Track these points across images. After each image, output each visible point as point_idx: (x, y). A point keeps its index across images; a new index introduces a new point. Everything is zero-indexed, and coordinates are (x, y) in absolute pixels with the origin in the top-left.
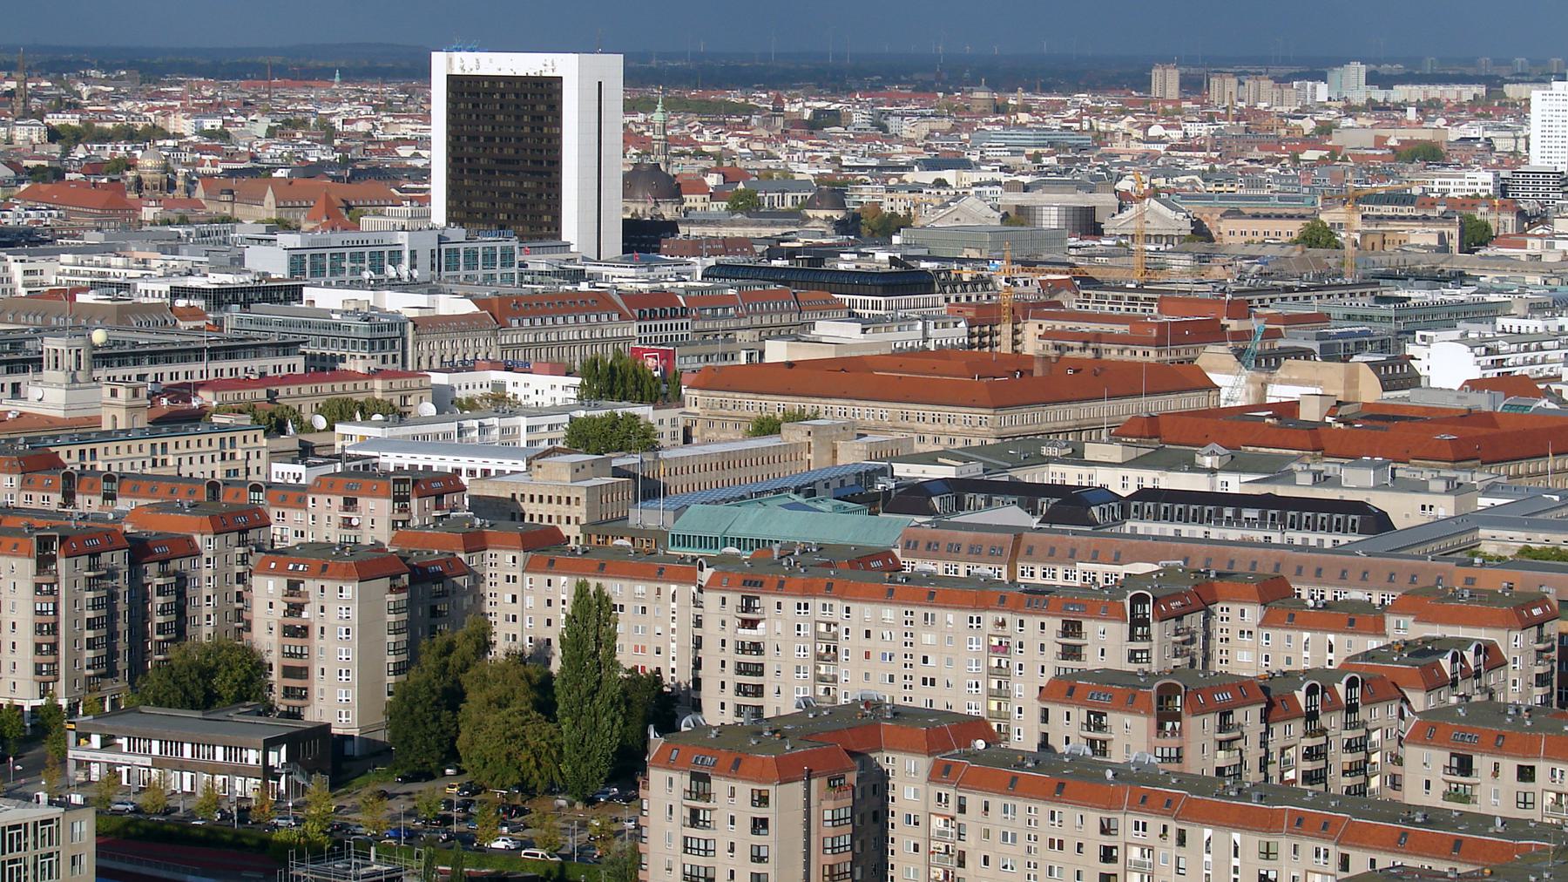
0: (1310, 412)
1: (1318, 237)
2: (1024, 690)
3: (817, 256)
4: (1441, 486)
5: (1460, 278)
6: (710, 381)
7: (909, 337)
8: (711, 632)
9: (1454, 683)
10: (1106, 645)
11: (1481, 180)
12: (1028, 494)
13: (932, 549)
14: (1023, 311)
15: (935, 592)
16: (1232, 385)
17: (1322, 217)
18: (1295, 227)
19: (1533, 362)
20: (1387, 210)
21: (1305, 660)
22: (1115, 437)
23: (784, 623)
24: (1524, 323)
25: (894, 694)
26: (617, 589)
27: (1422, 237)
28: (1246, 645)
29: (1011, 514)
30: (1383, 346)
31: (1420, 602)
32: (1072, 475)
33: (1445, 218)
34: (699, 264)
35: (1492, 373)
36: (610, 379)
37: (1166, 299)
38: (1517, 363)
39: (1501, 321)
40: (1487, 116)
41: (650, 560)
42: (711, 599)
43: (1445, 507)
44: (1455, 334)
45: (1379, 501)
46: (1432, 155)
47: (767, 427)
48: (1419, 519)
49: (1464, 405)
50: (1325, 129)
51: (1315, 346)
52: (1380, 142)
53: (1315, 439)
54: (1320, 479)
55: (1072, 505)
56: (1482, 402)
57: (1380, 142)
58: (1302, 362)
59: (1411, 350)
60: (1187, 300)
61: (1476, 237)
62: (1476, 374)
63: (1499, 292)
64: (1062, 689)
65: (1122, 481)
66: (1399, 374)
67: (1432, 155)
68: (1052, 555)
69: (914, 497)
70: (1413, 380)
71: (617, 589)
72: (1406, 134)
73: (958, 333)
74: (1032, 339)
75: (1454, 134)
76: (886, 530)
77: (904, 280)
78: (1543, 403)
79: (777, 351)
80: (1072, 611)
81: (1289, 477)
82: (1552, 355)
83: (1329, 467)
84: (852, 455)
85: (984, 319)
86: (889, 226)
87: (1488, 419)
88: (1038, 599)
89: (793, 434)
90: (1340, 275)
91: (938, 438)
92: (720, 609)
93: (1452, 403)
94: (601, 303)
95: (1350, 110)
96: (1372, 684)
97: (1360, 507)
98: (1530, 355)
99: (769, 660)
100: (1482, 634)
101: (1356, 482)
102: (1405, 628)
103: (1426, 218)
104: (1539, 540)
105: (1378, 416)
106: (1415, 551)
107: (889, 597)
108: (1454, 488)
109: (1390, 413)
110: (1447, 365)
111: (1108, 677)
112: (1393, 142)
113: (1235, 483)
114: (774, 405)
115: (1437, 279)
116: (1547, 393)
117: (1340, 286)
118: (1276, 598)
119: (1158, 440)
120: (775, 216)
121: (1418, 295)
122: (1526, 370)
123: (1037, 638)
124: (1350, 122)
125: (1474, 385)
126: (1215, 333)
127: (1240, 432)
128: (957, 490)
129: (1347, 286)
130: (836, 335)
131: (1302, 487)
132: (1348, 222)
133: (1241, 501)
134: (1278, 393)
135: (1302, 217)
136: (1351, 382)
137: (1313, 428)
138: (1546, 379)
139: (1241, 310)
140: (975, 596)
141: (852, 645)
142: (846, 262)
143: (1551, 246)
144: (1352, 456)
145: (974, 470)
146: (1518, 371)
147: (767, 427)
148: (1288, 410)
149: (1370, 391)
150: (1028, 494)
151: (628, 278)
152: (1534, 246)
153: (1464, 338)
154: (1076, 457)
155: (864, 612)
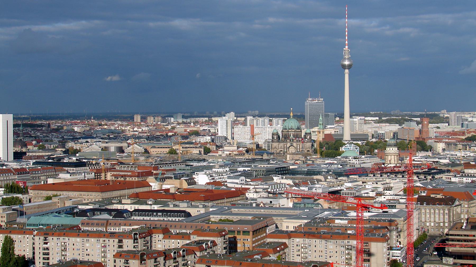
0: (172, 191)
1: (173, 152)
2: (110, 256)
3: (59, 159)
4: (202, 206)
5: (204, 160)
6: (35, 188)
7: (81, 177)
8: (37, 246)
9: (206, 250)
10: (128, 244)
11: (208, 139)
12: (109, 211)
13: (88, 224)
14: (107, 170)
15: (88, 234)
16: (155, 185)
17: (173, 147)
18: (167, 150)
19: (221, 178)
20: (188, 146)
21: (173, 246)
22: (129, 198)
23: (54, 243)
24: (218, 170)
25: (80, 258)
26: (14, 237)
27: (196, 151)
28: (160, 243)
29: (106, 216)
30: (188, 176)
31: (198, 232)
32: (119, 207)
33: (200, 147)
34: (32, 162)
35: (212, 181)
36: (11, 189)
37: (139, 167)
38: (217, 179)
39: (213, 170)
40: (209, 125)
41: (22, 230)
42: (37, 238)
43: (203, 211)
44: (204, 173)
45: (188, 210)
46: (197, 134)
47: (49, 198)
48: (197, 214)
49: (206, 188)
50: (173, 128)
51: (173, 176)
52: (185, 131)
53: (173, 197)
54: (175, 206)
55: (120, 214)
56: (210, 187)
57: (185, 131)
58: (170, 180)
59: (194, 176)
60: (144, 167)
61: (207, 151)
62: (208, 181)
63: (213, 163)
64: (119, 255)
65: (131, 208)
66: (191, 182)
67: (197, 134)
68: (115, 225)
69: (83, 213)
70: (195, 183)
71: (14, 237)
72: (191, 129)
73: (92, 176)
74: (109, 176)
75: (202, 128)
76: (77, 221)
77: (79, 164)
78: (223, 187)
79: (50, 181)
80: (120, 237)
81: (168, 206)
82: (225, 177)
83: (177, 203)
84: (68, 204)
85: (98, 172)
86: (75, 152)
87: (211, 191)
88: (112, 235)
89: (55, 200)
90: (178, 160)
91: (88, 200)
92: (39, 241)
93: (203, 188)
94: (9, 171)
95: (179, 124)
96: (188, 251)
97: (184, 212)
98: (220, 177)
99: (50, 251)
100: (212, 239)
101: (183, 206)
102: (195, 238)
103: (196, 147)
104: (223, 217)
105: (187, 191)
106: (196, 221)
107: (78, 236)
108: (204, 206)
109: (190, 190)
110: (202, 179)
111: (129, 252)
112: (188, 131)
113: (156, 207)
114: (50, 193)
115: (199, 160)
116: (224, 185)
117: (177, 163)
118: (166, 232)
119: (138, 198)
120: (49, 150)
121: (195, 164)
122: (219, 180)
123: (113, 243)
124: (179, 126)
125: (208, 184)
126: (150, 174)
127: (157, 196)
128: (93, 211)
129: (179, 163)
130: (64, 177)
131: (171, 208)
132: (179, 148)
133: (157, 211)
134: (165, 187)
135: (169, 148)
136: (181, 184)
137: (173, 194)
138: (224, 182)
139: (156, 168)
140: (98, 235)
141: (69, 247)
142: (66, 160)
143: (223, 153)
144: (182, 200)
145: (97, 206)
146: (218, 180)
147: (49, 198)
148: (167, 190)
149: (185, 186)
150: (109, 211)
151: (15, 165)
152: (220, 153)
153: (205, 173)
154: (120, 203)
155: (73, 239)
